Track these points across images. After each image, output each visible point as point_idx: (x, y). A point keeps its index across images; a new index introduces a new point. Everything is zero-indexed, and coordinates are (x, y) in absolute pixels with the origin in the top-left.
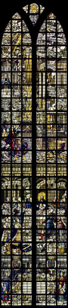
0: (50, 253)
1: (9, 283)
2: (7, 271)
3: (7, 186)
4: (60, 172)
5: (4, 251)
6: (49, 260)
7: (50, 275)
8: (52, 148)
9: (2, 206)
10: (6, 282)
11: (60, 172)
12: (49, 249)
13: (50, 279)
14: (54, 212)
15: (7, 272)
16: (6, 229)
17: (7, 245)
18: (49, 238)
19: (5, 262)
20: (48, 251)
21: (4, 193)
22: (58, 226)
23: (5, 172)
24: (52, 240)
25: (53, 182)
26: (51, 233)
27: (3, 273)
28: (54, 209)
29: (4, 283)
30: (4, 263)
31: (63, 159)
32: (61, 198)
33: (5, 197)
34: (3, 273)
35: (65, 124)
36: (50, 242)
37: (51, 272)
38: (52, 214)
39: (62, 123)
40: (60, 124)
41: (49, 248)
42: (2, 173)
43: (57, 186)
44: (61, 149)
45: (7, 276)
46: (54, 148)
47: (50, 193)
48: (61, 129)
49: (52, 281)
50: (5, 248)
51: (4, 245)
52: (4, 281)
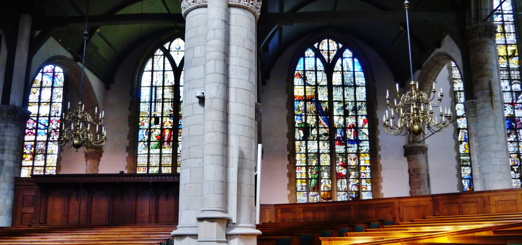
0: (512, 151)
1: (470, 181)
2: (467, 169)
3: (459, 88)
4: (514, 76)
5: (462, 149)
6: (512, 158)
7: (515, 172)
8: (503, 53)
9: (457, 106)
10: (467, 180)
11: (514, 76)
12: (511, 147)
13: (515, 176)
14: (512, 113)
15: (468, 170)
16: (463, 129)
17: (465, 144)
18: (509, 137)
19: (465, 160)
20: (509, 150)
21: (457, 94)
22: (518, 126)
23: (456, 75)
24: (513, 140)
25: (507, 84)
26: (511, 132)
27: (464, 171)
28: (511, 109)
29: (465, 180)
30: (464, 161)
31: (515, 63)
32: (517, 99)
33: (459, 98)
34: (464, 171)
35: (513, 33)
36: (511, 142)
37: (516, 170)
38: (510, 116)
39: (510, 32)
40: (508, 33)
41: (510, 147)
42: (454, 75)
43: (511, 88)
44: (512, 54)
45: (468, 174)
46: (504, 54)
47: (505, 94)
48: (510, 37)
49: (518, 179)
50: (463, 147)
51: (461, 144)
52: (465, 179)
